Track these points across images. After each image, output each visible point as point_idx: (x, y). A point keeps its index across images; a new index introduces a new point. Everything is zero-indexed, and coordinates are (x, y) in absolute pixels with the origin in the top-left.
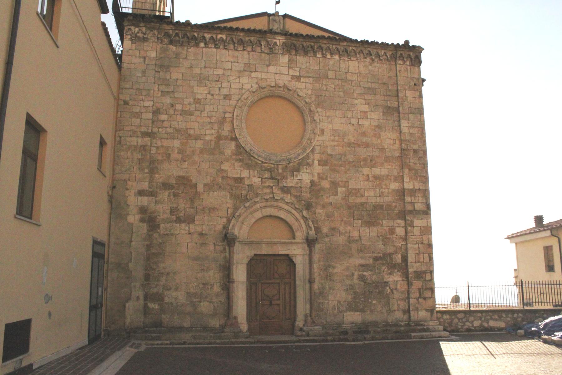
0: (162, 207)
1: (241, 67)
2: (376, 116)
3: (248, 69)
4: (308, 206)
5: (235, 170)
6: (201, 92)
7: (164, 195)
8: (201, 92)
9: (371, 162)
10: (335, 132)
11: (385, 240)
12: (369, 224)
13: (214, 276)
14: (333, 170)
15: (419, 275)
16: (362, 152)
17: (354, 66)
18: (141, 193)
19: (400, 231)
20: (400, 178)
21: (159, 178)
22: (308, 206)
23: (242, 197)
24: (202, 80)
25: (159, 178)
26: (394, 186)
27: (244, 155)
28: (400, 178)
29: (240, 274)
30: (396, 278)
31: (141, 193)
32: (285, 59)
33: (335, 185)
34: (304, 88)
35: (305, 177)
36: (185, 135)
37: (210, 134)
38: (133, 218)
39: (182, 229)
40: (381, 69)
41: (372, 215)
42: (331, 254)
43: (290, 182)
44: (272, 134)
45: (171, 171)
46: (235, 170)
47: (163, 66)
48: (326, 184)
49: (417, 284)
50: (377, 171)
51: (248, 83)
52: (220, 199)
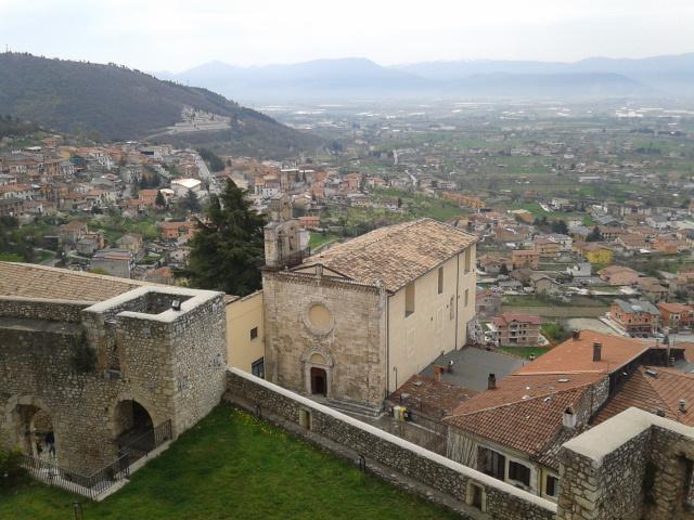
0: (281, 346)
1: (303, 292)
2: (358, 317)
3: (307, 293)
4: (330, 352)
5: (305, 335)
6: (291, 302)
7: (282, 341)
8: (291, 302)
9: (355, 338)
10: (341, 324)
11: (360, 371)
12: (354, 363)
13: (299, 372)
14: (340, 339)
15: (373, 388)
16: (352, 333)
17: (350, 294)
18: (274, 340)
19: (367, 369)
20: (367, 347)
21: (280, 334)
22: (330, 352)
23: (308, 346)
24: (291, 297)
25: (280, 334)
26: (365, 350)
27: (309, 333)
28: (367, 347)
29: (308, 373)
30: (364, 387)
31: (274, 340)
32: (321, 289)
33: (340, 346)
34: (329, 303)
35: (329, 341)
36: (288, 320)
37: (295, 320)
38: (272, 348)
39: (288, 353)
40: (361, 295)
41: (355, 361)
42: (339, 373)
43: (324, 342)
44: (319, 323)
45: (283, 332)
46: (305, 335)
47: (277, 291)
48: (337, 345)
49: (373, 391)
50: (359, 342)
51: (307, 299)
52: (299, 345)
